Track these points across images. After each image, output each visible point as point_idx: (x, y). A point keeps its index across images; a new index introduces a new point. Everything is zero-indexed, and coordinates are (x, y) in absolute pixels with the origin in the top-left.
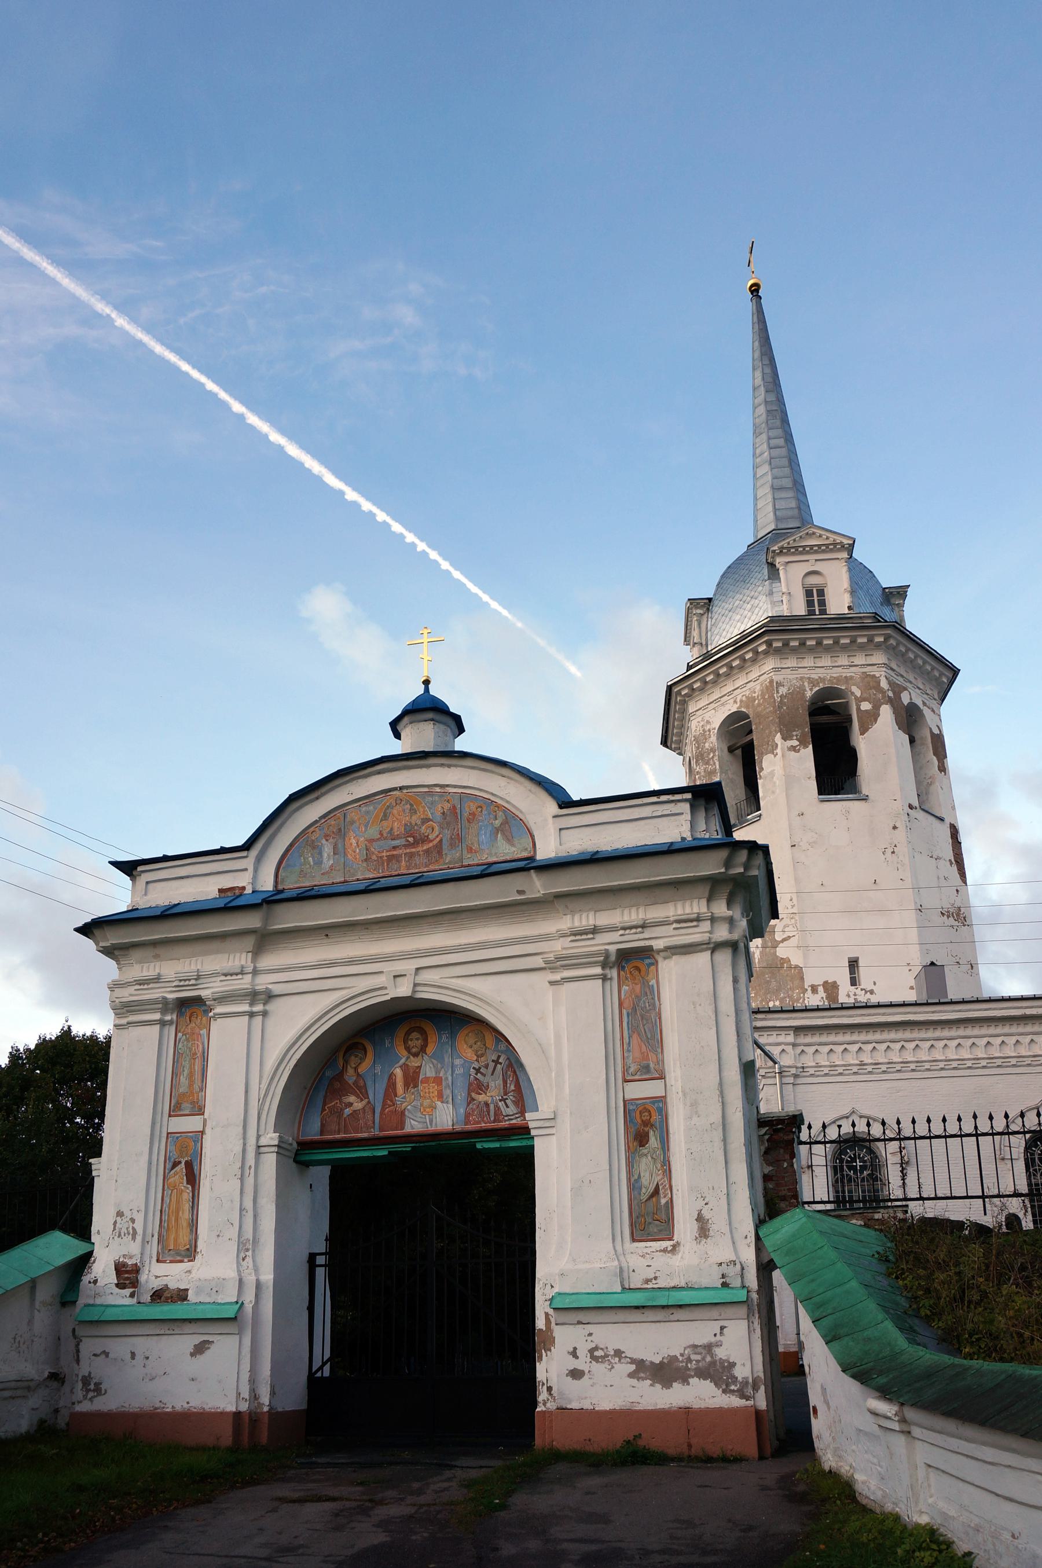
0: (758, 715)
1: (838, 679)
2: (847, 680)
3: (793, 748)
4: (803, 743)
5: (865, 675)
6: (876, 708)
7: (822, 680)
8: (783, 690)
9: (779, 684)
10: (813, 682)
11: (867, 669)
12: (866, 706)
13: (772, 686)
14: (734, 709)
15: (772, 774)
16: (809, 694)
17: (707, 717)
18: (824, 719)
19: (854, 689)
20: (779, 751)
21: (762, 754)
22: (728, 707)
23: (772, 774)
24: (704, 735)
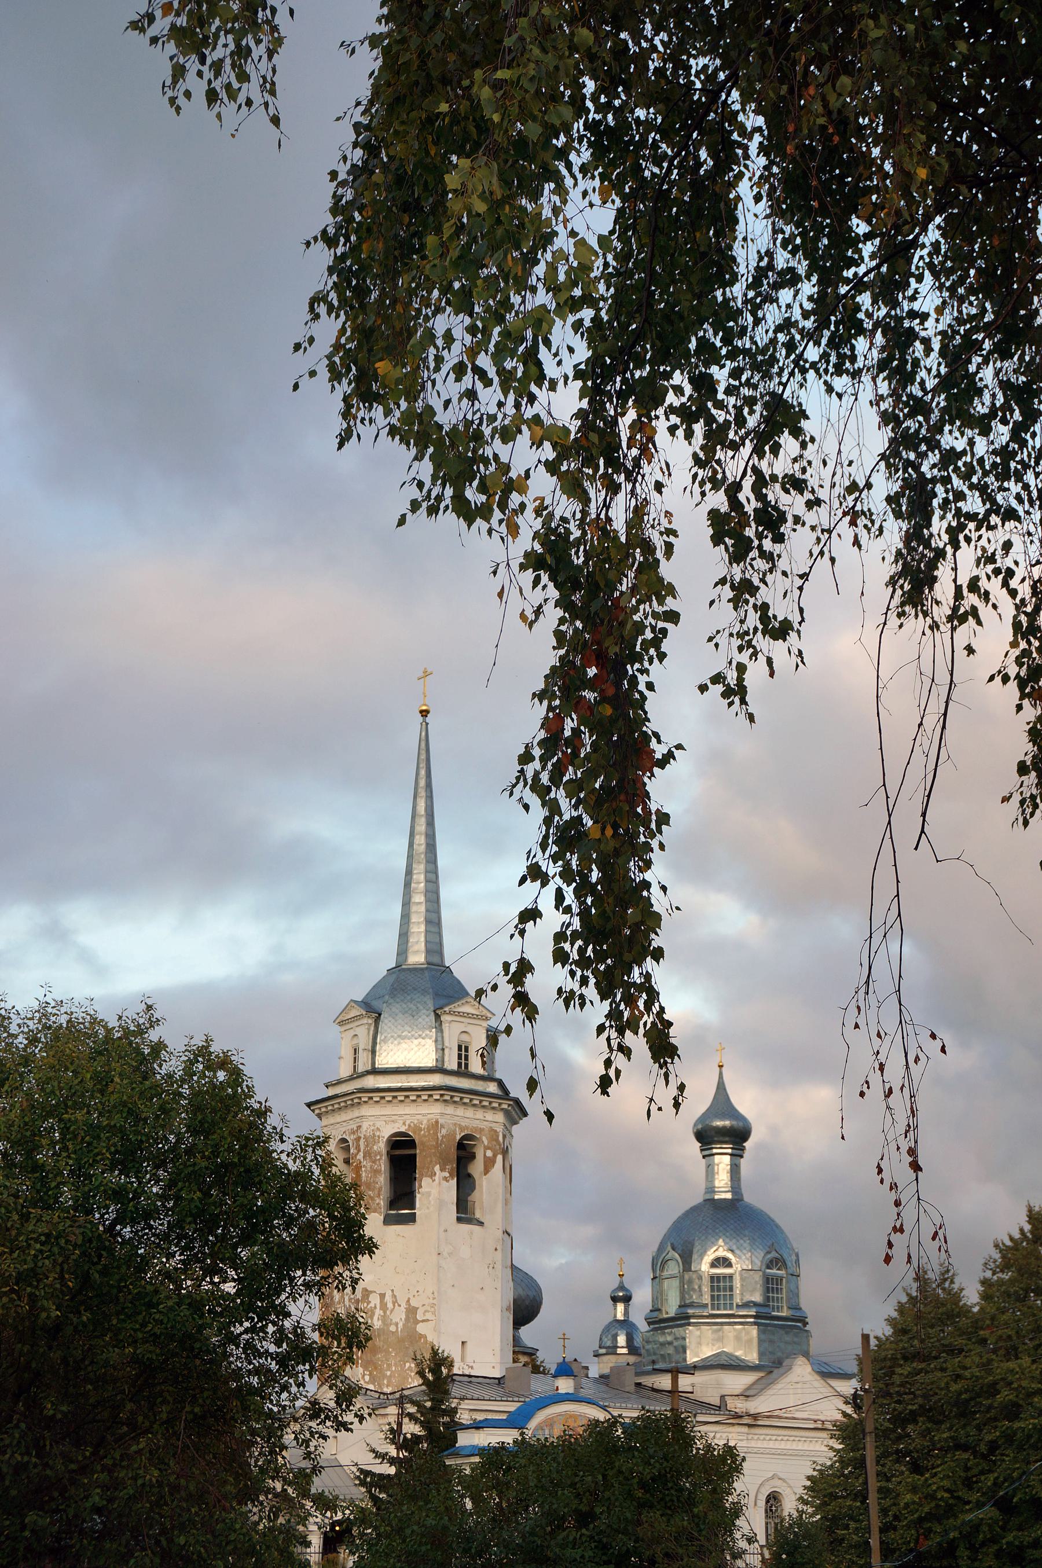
0: (423, 1143)
1: (476, 1129)
2: (481, 1130)
3: (445, 1179)
4: (451, 1175)
5: (492, 1130)
6: (495, 1156)
7: (467, 1128)
8: (444, 1131)
9: (442, 1126)
10: (462, 1129)
11: (493, 1125)
12: (489, 1154)
13: (436, 1125)
14: (403, 1129)
15: (429, 1194)
16: (458, 1137)
17: (378, 1124)
18: (463, 1153)
19: (484, 1139)
20: (437, 1178)
21: (422, 1176)
22: (397, 1125)
23: (429, 1194)
24: (372, 1139)
